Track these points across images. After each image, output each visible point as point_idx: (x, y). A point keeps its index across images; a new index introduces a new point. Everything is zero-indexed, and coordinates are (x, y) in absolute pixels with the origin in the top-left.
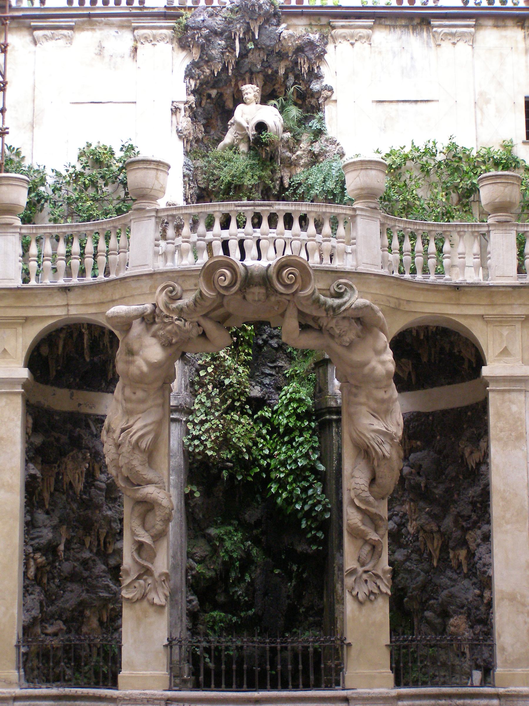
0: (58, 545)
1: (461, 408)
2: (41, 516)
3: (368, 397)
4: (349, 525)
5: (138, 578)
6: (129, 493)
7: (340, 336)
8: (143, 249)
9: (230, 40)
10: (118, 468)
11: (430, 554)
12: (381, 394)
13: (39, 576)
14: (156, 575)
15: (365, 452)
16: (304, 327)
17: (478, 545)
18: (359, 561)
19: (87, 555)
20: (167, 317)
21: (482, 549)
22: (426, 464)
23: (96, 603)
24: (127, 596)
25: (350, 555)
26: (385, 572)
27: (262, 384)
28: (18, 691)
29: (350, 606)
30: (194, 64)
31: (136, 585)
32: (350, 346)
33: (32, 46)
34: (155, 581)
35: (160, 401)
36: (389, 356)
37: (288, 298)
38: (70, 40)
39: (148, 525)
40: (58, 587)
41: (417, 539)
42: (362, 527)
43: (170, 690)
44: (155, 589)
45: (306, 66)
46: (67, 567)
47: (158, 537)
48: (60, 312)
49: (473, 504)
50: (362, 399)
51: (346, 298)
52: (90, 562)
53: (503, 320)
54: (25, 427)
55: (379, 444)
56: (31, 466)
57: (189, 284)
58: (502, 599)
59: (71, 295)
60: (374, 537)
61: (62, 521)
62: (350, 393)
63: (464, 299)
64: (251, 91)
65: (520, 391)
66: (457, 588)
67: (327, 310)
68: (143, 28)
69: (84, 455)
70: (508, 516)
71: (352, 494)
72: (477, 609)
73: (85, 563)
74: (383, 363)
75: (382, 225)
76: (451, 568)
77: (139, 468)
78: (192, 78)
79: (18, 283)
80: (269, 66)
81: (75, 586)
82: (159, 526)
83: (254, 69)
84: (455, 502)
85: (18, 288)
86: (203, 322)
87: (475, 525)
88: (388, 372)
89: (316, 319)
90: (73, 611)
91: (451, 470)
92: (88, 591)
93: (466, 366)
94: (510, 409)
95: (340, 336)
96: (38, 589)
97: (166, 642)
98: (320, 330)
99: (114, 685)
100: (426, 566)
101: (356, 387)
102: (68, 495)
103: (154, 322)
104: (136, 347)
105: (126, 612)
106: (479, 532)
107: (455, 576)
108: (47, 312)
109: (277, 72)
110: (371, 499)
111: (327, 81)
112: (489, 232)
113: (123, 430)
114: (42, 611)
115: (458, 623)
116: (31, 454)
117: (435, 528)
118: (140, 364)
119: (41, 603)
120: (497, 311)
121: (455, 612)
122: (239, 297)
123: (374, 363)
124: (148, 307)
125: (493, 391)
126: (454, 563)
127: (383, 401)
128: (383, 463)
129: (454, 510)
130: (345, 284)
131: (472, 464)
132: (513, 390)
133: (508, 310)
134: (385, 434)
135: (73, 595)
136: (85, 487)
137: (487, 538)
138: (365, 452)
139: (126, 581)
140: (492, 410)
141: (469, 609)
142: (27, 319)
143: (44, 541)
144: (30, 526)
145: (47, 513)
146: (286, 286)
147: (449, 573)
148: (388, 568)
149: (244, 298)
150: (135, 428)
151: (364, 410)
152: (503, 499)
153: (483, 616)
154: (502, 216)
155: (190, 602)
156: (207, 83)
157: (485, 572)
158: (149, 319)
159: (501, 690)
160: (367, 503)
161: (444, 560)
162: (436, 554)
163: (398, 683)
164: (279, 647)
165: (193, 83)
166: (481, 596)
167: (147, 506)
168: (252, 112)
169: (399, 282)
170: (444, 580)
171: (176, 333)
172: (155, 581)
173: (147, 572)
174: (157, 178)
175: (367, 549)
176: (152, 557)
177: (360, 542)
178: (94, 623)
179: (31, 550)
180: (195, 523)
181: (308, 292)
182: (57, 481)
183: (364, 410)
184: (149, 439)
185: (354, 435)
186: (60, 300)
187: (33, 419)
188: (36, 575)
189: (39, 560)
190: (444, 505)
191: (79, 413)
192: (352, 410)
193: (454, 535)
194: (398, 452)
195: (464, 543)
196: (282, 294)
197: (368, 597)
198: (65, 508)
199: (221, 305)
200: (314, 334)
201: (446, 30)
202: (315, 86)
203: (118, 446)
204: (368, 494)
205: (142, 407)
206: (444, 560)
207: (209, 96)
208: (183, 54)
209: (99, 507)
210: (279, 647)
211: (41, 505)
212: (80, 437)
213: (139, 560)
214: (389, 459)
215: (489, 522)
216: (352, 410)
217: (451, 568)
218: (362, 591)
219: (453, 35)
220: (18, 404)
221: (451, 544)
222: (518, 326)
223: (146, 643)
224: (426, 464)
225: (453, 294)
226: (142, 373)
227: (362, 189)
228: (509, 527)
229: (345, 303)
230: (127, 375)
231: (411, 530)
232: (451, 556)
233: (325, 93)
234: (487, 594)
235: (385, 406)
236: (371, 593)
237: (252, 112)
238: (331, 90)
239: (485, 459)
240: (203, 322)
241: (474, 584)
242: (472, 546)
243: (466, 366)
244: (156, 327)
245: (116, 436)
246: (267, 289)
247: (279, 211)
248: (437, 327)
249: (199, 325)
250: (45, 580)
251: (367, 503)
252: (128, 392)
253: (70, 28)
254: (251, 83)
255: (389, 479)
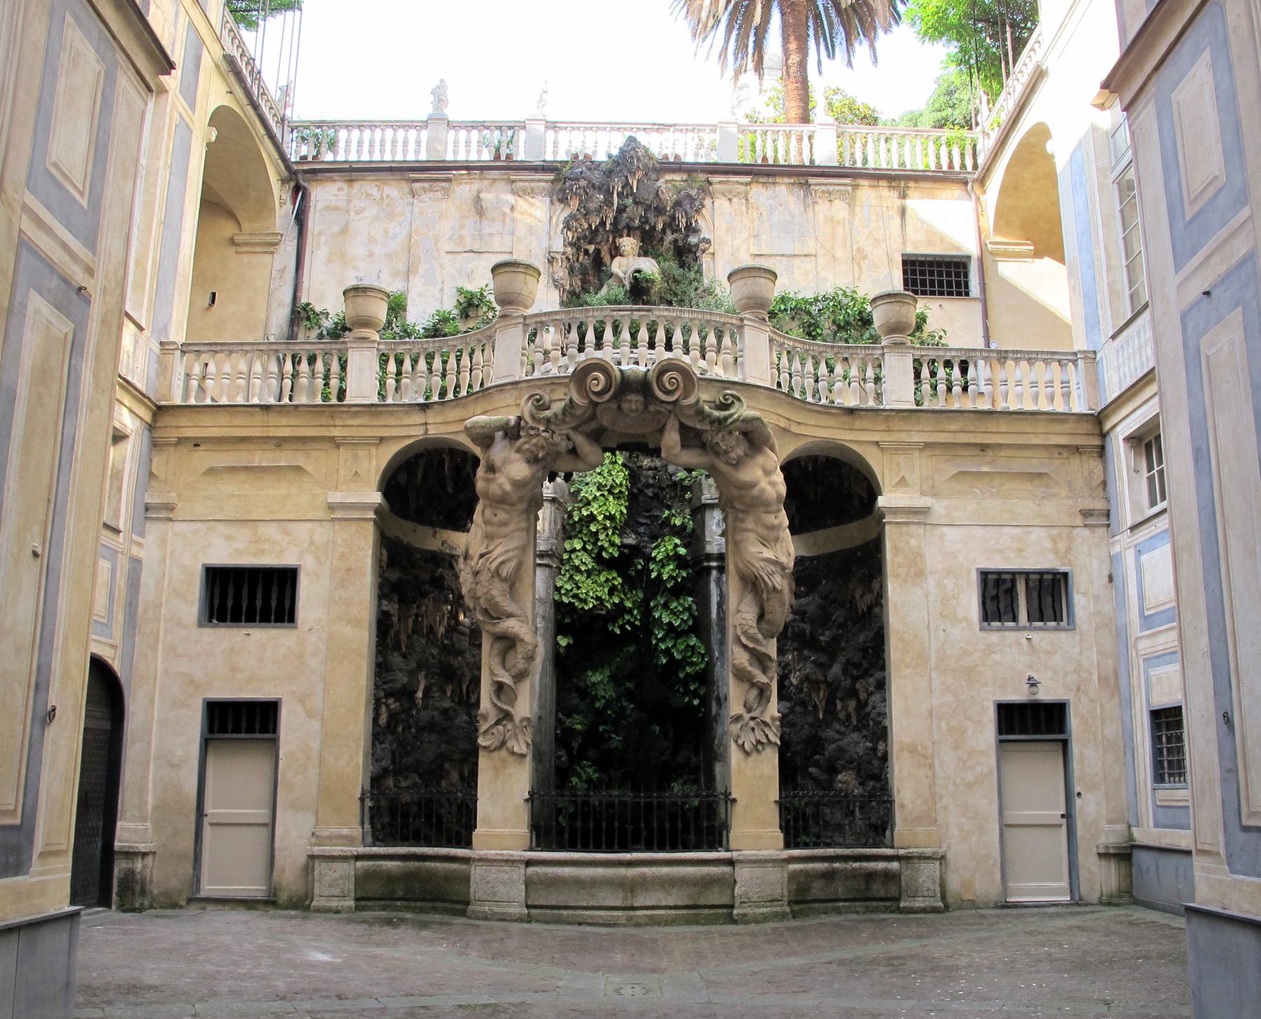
0: (415, 692)
1: (850, 550)
2: (396, 659)
3: (755, 522)
4: (734, 666)
5: (498, 723)
6: (487, 627)
7: (726, 452)
8: (507, 359)
9: (609, 194)
10: (476, 599)
11: (815, 706)
12: (771, 519)
13: (393, 724)
14: (517, 720)
15: (752, 584)
16: (684, 446)
17: (870, 694)
18: (745, 706)
19: (447, 704)
20: (532, 428)
21: (876, 698)
22: (811, 609)
23: (457, 756)
24: (484, 744)
25: (735, 698)
26: (773, 719)
27: (637, 533)
28: (362, 850)
29: (735, 755)
30: (573, 217)
31: (494, 731)
32: (737, 464)
33: (409, 199)
34: (515, 727)
35: (524, 525)
36: (779, 477)
37: (669, 407)
38: (447, 192)
39: (508, 665)
40: (414, 737)
41: (801, 691)
42: (750, 668)
43: (531, 849)
44: (516, 735)
45: (684, 221)
46: (425, 716)
47: (520, 676)
48: (418, 432)
49: (864, 650)
50: (750, 524)
51: (732, 411)
52: (451, 712)
53: (903, 448)
54: (378, 560)
55: (770, 575)
56: (384, 602)
57: (559, 393)
58: (902, 750)
59: (429, 412)
60: (762, 679)
61: (420, 667)
62: (736, 519)
63: (858, 424)
64: (629, 243)
65: (919, 523)
66: (846, 741)
67: (712, 423)
68: (521, 180)
69: (447, 597)
70: (907, 659)
71: (739, 631)
72: (869, 763)
73: (445, 712)
74: (773, 484)
75: (771, 340)
76: (839, 720)
77: (499, 599)
78: (569, 229)
79: (375, 400)
80: (647, 222)
81: (434, 737)
82: (521, 665)
83: (632, 224)
84: (844, 649)
85: (372, 405)
86: (573, 435)
87: (866, 674)
88: (779, 496)
89: (698, 434)
90: (431, 762)
91: (838, 616)
92: (448, 743)
93: (856, 502)
94: (908, 543)
95: (726, 452)
96: (390, 738)
97: (527, 796)
98: (703, 446)
99: (468, 844)
100: (810, 719)
101: (743, 511)
102: (428, 640)
103: (519, 437)
104: (498, 463)
105: (484, 762)
106: (871, 680)
107: (843, 729)
108: (404, 432)
109: (654, 228)
110: (760, 636)
111: (705, 234)
112: (883, 355)
113: (482, 556)
114: (393, 761)
115: (846, 779)
116: (386, 590)
117: (821, 678)
118: (502, 483)
119: (393, 752)
120: (894, 437)
121: (844, 768)
122: (614, 406)
123: (764, 484)
124: (513, 419)
125: (890, 523)
126: (842, 715)
127: (772, 528)
128: (772, 596)
129: (842, 659)
130: (732, 396)
131: (862, 606)
132: (912, 523)
133: (904, 437)
134: (776, 563)
135: (430, 747)
136: (447, 631)
137: (882, 685)
138: (752, 584)
139: (484, 727)
140: (888, 545)
141: (859, 764)
142: (382, 439)
143: (398, 685)
144: (382, 669)
145: (404, 656)
146: (668, 392)
147: (837, 726)
148: (778, 715)
149: (620, 408)
150: (495, 553)
151: (752, 536)
152: (901, 640)
153: (876, 772)
154: (897, 338)
155: (559, 757)
156: (585, 237)
157: (880, 722)
158: (512, 432)
159: (902, 852)
160: (756, 641)
161: (831, 711)
162: (821, 706)
163: (787, 845)
164: (655, 802)
165: (570, 234)
166: (874, 749)
167: (508, 642)
168: (630, 261)
169: (790, 400)
170: (831, 734)
171: (543, 447)
172: (515, 727)
173: (506, 716)
174: (525, 283)
175: (754, 692)
176: (513, 700)
177: (746, 686)
178: (455, 777)
179: (382, 694)
180: (566, 668)
181: (692, 400)
182: (416, 622)
183: (752, 536)
184: (515, 571)
185: (741, 565)
186: (418, 418)
187: (388, 552)
188: (389, 723)
189: (392, 706)
190: (832, 651)
191: (441, 552)
192: (738, 537)
193: (843, 684)
194: (790, 585)
195: (853, 693)
196: (663, 402)
197: (755, 747)
198: (424, 652)
199: (593, 417)
200: (698, 451)
201: (823, 188)
202: (693, 240)
203: (476, 574)
204: (756, 631)
205: (504, 530)
206: (831, 711)
207: (586, 252)
208: (559, 207)
209: (460, 653)
210: (655, 802)
211: (397, 647)
212: (442, 577)
213: (499, 704)
214: (780, 592)
215: (883, 668)
216: (738, 537)
217: (839, 720)
218: (749, 740)
219: (830, 193)
220: (370, 529)
221: (839, 694)
222: (916, 454)
223: (504, 796)
224: (811, 609)
225: (846, 419)
226: (504, 490)
227: (749, 298)
228: (908, 671)
229: (731, 415)
230: (487, 496)
231: (794, 681)
232: (839, 707)
233: (702, 246)
234: (881, 746)
235: (773, 534)
236: (759, 742)
237: (630, 261)
238: (708, 242)
239: (879, 598)
240: (573, 435)
241: (865, 737)
242: (863, 696)
243: (856, 502)
244: (521, 440)
245: (473, 563)
246: (645, 398)
247: (659, 317)
248: (827, 458)
249: (569, 439)
250: (400, 729)
251: (756, 641)
252: (488, 512)
253: (448, 180)
254: (629, 235)
255: (781, 613)
